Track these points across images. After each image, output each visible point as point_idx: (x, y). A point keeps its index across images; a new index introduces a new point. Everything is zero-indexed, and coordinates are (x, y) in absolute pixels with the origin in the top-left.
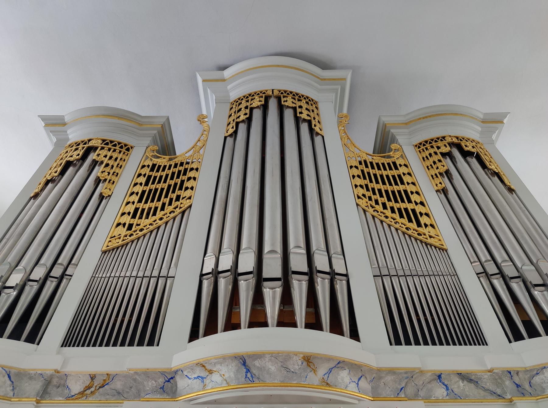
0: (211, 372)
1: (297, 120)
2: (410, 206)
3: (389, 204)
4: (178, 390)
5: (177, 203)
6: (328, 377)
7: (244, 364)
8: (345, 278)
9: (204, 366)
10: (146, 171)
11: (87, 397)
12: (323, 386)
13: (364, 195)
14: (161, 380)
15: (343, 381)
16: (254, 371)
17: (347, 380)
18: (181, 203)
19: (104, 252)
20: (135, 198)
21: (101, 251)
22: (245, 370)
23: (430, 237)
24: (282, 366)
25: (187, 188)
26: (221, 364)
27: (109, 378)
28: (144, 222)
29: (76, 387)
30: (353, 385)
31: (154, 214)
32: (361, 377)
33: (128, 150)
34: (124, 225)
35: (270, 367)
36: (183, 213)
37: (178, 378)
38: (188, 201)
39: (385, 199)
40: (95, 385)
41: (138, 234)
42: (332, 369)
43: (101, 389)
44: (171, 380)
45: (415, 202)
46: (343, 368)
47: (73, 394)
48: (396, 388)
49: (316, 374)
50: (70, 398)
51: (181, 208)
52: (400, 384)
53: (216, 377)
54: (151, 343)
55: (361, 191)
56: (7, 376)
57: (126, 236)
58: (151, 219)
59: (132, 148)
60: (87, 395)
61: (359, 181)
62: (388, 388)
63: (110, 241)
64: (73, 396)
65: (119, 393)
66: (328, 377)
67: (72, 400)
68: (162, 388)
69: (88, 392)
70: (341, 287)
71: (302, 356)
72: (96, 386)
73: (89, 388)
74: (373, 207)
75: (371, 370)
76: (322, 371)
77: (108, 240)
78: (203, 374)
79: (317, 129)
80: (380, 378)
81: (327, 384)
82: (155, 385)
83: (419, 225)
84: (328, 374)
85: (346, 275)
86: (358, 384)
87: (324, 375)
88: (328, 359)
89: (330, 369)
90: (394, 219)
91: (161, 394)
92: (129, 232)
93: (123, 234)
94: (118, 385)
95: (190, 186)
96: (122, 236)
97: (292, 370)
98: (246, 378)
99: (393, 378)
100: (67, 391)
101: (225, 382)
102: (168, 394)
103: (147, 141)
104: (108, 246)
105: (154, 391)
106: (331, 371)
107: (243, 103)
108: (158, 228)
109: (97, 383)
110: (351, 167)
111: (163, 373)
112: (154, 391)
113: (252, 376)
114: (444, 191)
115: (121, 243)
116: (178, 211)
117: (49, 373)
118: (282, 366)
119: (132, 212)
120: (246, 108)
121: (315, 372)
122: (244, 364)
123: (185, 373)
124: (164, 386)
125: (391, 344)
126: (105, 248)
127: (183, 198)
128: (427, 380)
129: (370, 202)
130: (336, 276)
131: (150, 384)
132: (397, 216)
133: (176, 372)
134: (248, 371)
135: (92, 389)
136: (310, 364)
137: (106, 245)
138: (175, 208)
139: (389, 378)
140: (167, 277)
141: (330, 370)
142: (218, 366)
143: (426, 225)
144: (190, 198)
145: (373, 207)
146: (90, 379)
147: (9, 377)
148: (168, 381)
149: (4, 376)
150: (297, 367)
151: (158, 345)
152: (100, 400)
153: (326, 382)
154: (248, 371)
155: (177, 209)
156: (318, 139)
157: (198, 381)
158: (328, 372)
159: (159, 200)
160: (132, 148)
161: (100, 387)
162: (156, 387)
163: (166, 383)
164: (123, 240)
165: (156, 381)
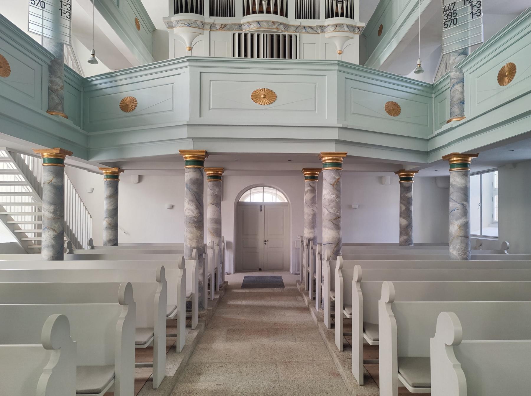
0: (251, 25)
7: (259, 23)
9: (249, 23)
22: (259, 24)
26: (253, 23)
37: (242, 26)
46: (281, 25)
53: (252, 26)
71: (272, 22)
78: (249, 25)
105: (237, 29)
109: (223, 26)
111: (239, 24)
117: (212, 23)
122: (259, 23)
123: (244, 25)
133: (242, 24)
134: (260, 25)
142: (253, 23)
157: (248, 27)
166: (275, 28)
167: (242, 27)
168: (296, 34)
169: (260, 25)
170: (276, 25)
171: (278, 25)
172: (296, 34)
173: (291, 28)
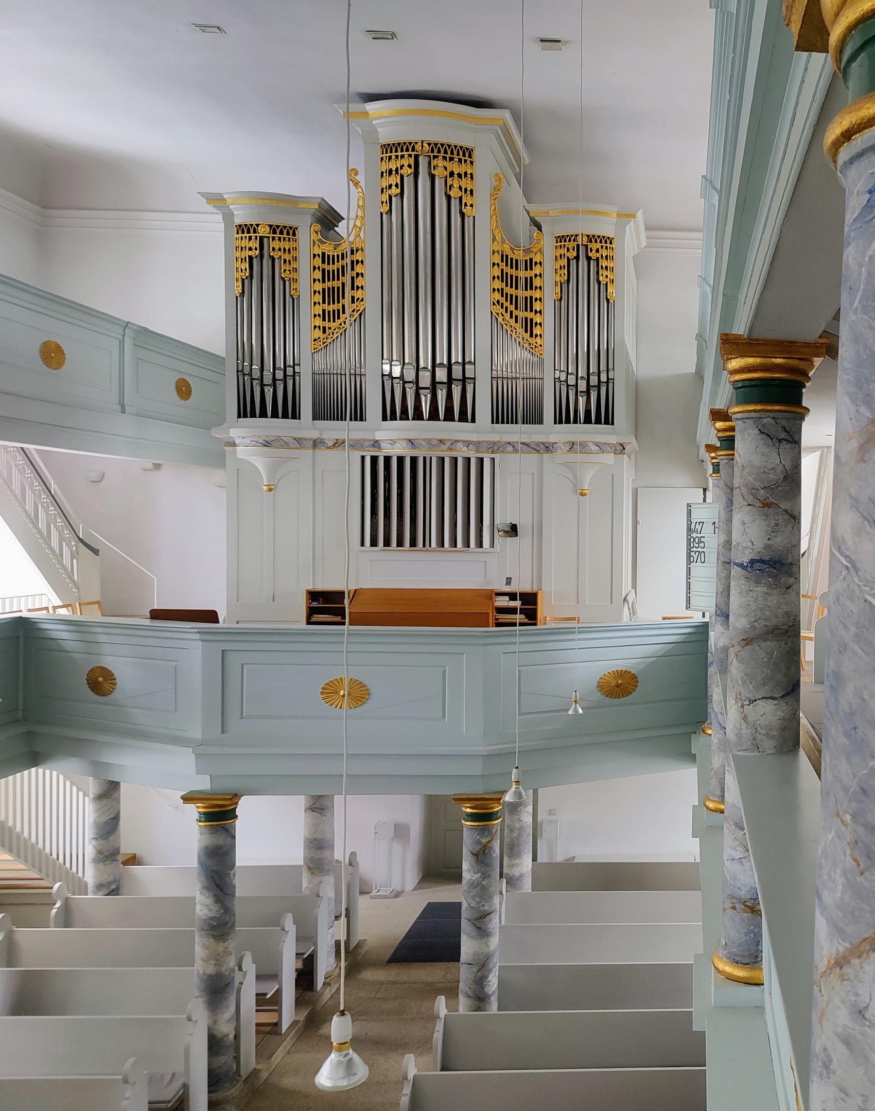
1: (449, 198)
2: (529, 315)
3: (515, 313)
5: (354, 306)
8: (473, 381)
10: (318, 262)
13: (498, 302)
18: (357, 306)
20: (318, 298)
23: (535, 346)
25: (358, 288)
28: (332, 324)
29: (330, 444)
31: (339, 318)
33: (294, 234)
34: (319, 327)
36: (360, 315)
38: (361, 302)
39: (512, 308)
45: (536, 310)
50: (328, 448)
51: (358, 311)
55: (497, 296)
57: (324, 339)
58: (338, 322)
59: (296, 228)
61: (498, 284)
69: (337, 445)
73: (336, 443)
74: (503, 315)
77: (313, 343)
79: (467, 210)
83: (531, 336)
85: (474, 379)
90: (515, 329)
92: (325, 336)
95: (360, 286)
96: (321, 339)
100: (325, 445)
103: (309, 219)
105: (370, 446)
107: (393, 157)
108: (345, 330)
110: (494, 264)
112: (370, 446)
114: (561, 299)
115: (322, 346)
116: (357, 315)
119: (321, 314)
120: (397, 170)
125: (493, 423)
126: (313, 351)
127: (358, 299)
129: (501, 310)
130: (467, 380)
132: (518, 326)
137: (313, 349)
138: (353, 311)
140: (361, 375)
143: (536, 335)
144: (362, 300)
145: (503, 315)
151: (365, 421)
155: (355, 312)
156: (468, 222)
159: (338, 302)
160: (296, 228)
164: (324, 343)
166: (445, 449)
168: (493, 456)
169: (412, 444)
170: (448, 444)
171: (452, 443)
172: (493, 456)
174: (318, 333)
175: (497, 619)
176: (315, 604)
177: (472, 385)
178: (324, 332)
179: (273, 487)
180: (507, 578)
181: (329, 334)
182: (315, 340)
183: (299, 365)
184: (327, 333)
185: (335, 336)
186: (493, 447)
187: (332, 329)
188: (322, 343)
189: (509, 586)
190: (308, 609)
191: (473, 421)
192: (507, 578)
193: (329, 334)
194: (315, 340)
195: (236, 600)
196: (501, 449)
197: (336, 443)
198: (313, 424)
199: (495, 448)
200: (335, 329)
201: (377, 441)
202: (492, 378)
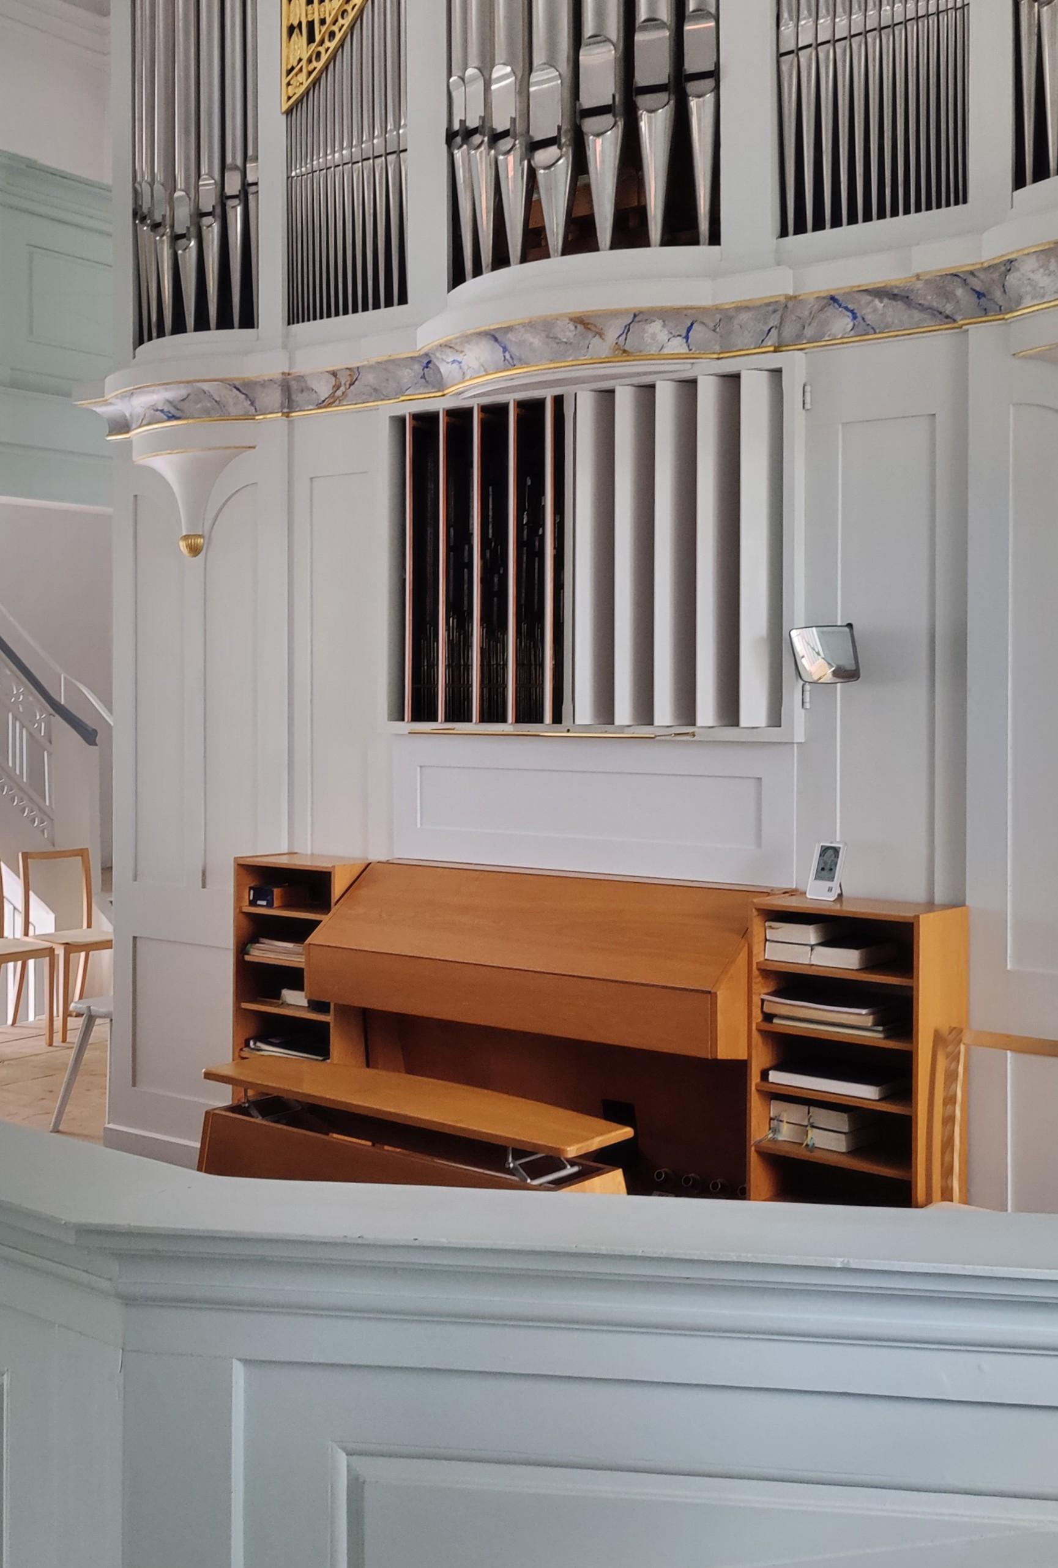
4: (444, 377)
6: (626, 339)
8: (710, 83)
11: (340, 400)
12: (616, 356)
14: (417, 367)
15: (654, 340)
16: (513, 349)
17: (663, 336)
19: (289, 112)
21: (283, 113)
24: (547, 337)
27: (354, 375)
30: (679, 341)
32: (692, 324)
35: (532, 340)
40: (343, 383)
41: (343, 26)
42: (629, 325)
43: (352, 387)
44: (430, 365)
47: (323, 399)
48: (761, 330)
49: (603, 339)
50: (320, 405)
52: (765, 323)
54: (403, 300)
56: (235, 390)
57: (310, 61)
60: (338, 397)
62: (746, 332)
63: (289, 84)
64: (324, 401)
65: (375, 390)
66: (626, 339)
67: (325, 407)
68: (423, 377)
69: (339, 393)
70: (699, 110)
72: (345, 384)
75: (704, 310)
76: (613, 332)
80: (731, 318)
81: (625, 351)
82: (413, 374)
84: (624, 335)
85: (714, 74)
86: (687, 338)
87: (619, 337)
88: (615, 314)
89: (626, 327)
91: (425, 387)
93: (305, 57)
94: (369, 378)
96: (304, 63)
97: (565, 340)
98: (504, 360)
99: (751, 315)
101: (482, 369)
102: (434, 387)
104: (289, 98)
106: (629, 330)
113: (511, 357)
118: (547, 337)
121: (601, 337)
124: (424, 374)
126: (285, 107)
128: (816, 307)
131: (406, 373)
135: (342, 389)
136: (589, 326)
137: (284, 98)
139: (744, 316)
141: (628, 328)
146: (332, 376)
147: (238, 389)
148: (427, 367)
149: (231, 390)
150: (570, 335)
152: (356, 404)
153: (622, 348)
154: (505, 350)
158: (623, 333)
161: (351, 385)
162: (415, 376)
163: (425, 369)
164: (310, 73)
165: (411, 369)
167: (435, 364)
173: (736, 322)
174: (300, 46)
175: (768, 1017)
176: (262, 909)
177: (710, 97)
178: (311, 39)
179: (200, 541)
180: (825, 850)
181: (322, 42)
182: (289, 72)
183: (256, 159)
184: (318, 38)
185: (338, 36)
186: (779, 327)
187: (328, 21)
188: (303, 75)
189: (829, 884)
190: (245, 922)
191: (715, 238)
192: (825, 850)
193: (322, 42)
194: (289, 72)
195: (131, 875)
196: (809, 332)
197: (339, 388)
198: (287, 336)
199: (789, 331)
200: (335, 22)
201: (428, 362)
202: (780, 55)
